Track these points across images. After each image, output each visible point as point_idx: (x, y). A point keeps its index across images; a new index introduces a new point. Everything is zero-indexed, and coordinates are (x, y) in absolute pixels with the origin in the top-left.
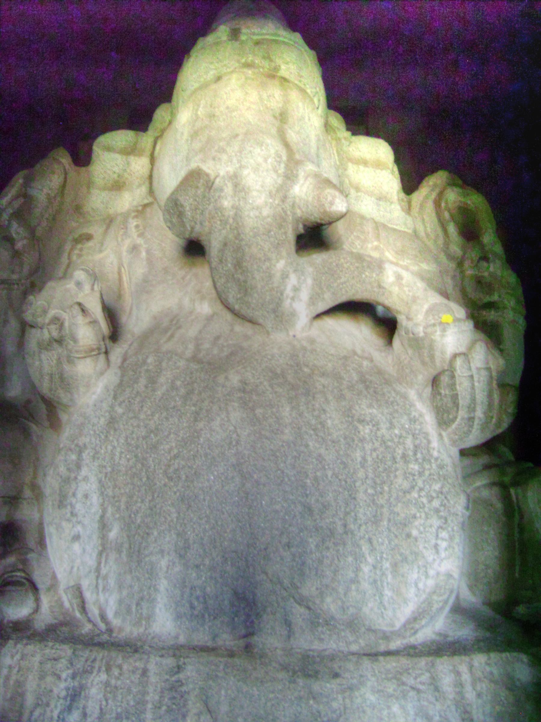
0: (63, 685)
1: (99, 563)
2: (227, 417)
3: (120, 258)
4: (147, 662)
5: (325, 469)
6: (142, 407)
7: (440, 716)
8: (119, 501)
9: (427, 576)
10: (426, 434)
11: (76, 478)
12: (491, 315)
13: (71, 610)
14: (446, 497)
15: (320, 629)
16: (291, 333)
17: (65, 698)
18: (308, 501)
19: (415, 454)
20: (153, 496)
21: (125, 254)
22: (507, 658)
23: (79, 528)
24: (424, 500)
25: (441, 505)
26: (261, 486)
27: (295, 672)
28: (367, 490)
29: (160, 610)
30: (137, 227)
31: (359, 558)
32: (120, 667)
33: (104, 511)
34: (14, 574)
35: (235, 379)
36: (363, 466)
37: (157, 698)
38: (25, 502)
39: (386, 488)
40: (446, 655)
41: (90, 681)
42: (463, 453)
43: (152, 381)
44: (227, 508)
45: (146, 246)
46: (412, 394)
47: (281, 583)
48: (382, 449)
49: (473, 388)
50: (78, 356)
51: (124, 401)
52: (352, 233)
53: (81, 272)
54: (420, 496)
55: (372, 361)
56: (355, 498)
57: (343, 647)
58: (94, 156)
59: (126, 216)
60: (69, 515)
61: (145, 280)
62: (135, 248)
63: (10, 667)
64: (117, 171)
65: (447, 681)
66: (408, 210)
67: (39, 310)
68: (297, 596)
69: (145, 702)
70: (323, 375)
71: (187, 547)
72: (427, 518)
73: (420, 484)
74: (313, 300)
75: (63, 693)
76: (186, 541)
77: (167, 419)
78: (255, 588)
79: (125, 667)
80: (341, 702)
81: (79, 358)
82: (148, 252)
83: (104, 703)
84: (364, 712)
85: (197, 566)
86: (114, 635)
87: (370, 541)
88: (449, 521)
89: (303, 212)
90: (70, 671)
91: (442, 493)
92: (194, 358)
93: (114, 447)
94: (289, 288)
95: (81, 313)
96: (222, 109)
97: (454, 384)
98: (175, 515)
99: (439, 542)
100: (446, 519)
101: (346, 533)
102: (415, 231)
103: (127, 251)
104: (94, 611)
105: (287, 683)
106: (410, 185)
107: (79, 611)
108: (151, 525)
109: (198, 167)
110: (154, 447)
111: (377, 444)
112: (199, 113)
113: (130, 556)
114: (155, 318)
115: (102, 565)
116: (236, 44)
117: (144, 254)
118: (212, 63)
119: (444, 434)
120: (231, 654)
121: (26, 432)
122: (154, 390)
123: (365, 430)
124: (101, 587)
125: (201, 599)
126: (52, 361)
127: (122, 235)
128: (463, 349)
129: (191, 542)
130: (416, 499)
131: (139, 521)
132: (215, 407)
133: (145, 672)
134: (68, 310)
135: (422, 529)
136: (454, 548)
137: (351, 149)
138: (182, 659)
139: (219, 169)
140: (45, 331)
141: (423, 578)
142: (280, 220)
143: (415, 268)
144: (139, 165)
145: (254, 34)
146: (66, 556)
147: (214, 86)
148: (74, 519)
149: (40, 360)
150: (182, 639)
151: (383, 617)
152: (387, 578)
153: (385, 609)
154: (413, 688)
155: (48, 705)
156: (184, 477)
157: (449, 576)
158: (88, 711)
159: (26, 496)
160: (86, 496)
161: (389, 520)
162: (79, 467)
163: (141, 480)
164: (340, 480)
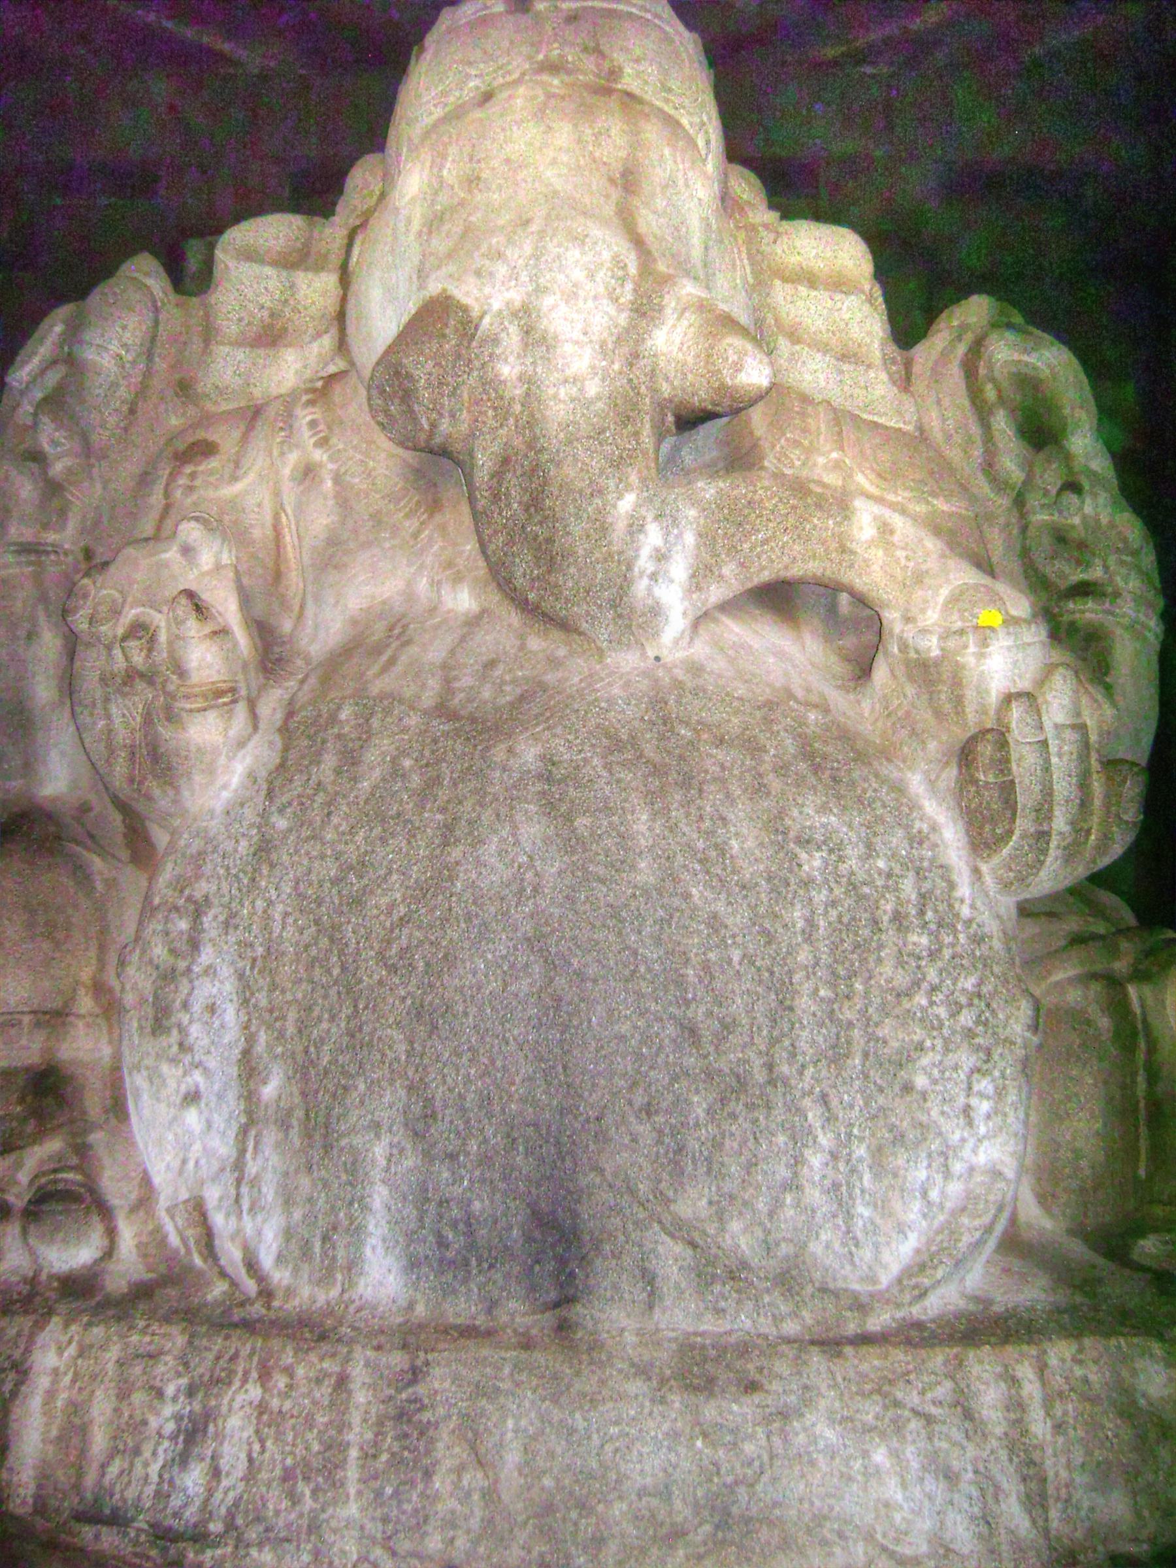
0: (168, 1410)
1: (242, 1152)
2: (514, 835)
3: (277, 494)
4: (347, 1359)
5: (726, 946)
6: (329, 814)
7: (976, 1472)
8: (284, 1018)
9: (947, 1174)
11: (189, 970)
12: (1087, 611)
13: (183, 1251)
14: (988, 1005)
15: (717, 1288)
16: (651, 653)
17: (173, 1438)
18: (690, 1014)
19: (922, 913)
20: (355, 1006)
22: (1119, 1348)
23: (198, 1077)
24: (942, 1012)
25: (978, 1022)
26: (589, 984)
27: (663, 1381)
28: (816, 990)
29: (374, 1248)
30: (313, 424)
31: (800, 1136)
32: (289, 1371)
33: (251, 1040)
34: (60, 1176)
35: (529, 754)
36: (808, 938)
37: (369, 1435)
38: (81, 1024)
39: (858, 986)
40: (988, 1343)
41: (225, 1402)
42: (1025, 911)
43: (350, 759)
44: (516, 1032)
46: (916, 782)
47: (632, 1192)
48: (848, 902)
49: (1047, 768)
50: (188, 706)
51: (290, 804)
52: (784, 434)
53: (193, 524)
54: (932, 1003)
55: (827, 711)
56: (791, 1009)
57: (765, 1325)
58: (218, 272)
59: (289, 402)
60: (175, 1048)
61: (333, 541)
62: (308, 472)
63: (56, 1372)
65: (990, 1400)
66: (905, 382)
67: (103, 609)
68: (667, 1218)
69: (344, 1447)
70: (720, 742)
71: (430, 1115)
72: (947, 1050)
73: (932, 975)
75: (170, 1426)
76: (429, 1101)
77: (383, 840)
78: (578, 1201)
79: (300, 1371)
80: (764, 1442)
81: (191, 711)
82: (337, 479)
83: (257, 1447)
84: (812, 1463)
85: (453, 1157)
86: (276, 1304)
87: (824, 1099)
88: (996, 1057)
89: (674, 388)
90: (184, 1381)
91: (979, 996)
92: (443, 710)
93: (270, 903)
94: (645, 552)
96: (495, 163)
97: (1008, 761)
98: (402, 1047)
99: (974, 1101)
100: (989, 1054)
101: (772, 1082)
103: (292, 479)
104: (231, 1254)
105: (647, 1404)
106: (908, 326)
107: (200, 1253)
108: (353, 1069)
109: (445, 290)
110: (357, 902)
111: (838, 891)
113: (308, 1135)
114: (354, 622)
115: (249, 1156)
116: (525, 20)
117: (329, 483)
119: (984, 868)
120: (527, 1344)
122: (355, 779)
123: (813, 862)
124: (246, 1204)
125: (461, 1226)
126: (134, 719)
127: (282, 443)
128: (1025, 685)
129: (438, 1104)
130: (923, 1009)
132: (487, 816)
133: (342, 1381)
134: (165, 609)
135: (936, 1072)
136: (1005, 1115)
137: (779, 251)
138: (421, 1354)
139: (490, 295)
141: (939, 1178)
142: (624, 410)
143: (920, 508)
144: (316, 289)
146: (171, 1137)
148: (188, 1059)
149: (109, 717)
151: (852, 1263)
152: (861, 1179)
153: (857, 1246)
154: (916, 1413)
155: (137, 1451)
157: (996, 1174)
158: (224, 1464)
159: (83, 1011)
160: (212, 1009)
161: (866, 1055)
162: (195, 945)
163: (329, 971)
164: (759, 970)
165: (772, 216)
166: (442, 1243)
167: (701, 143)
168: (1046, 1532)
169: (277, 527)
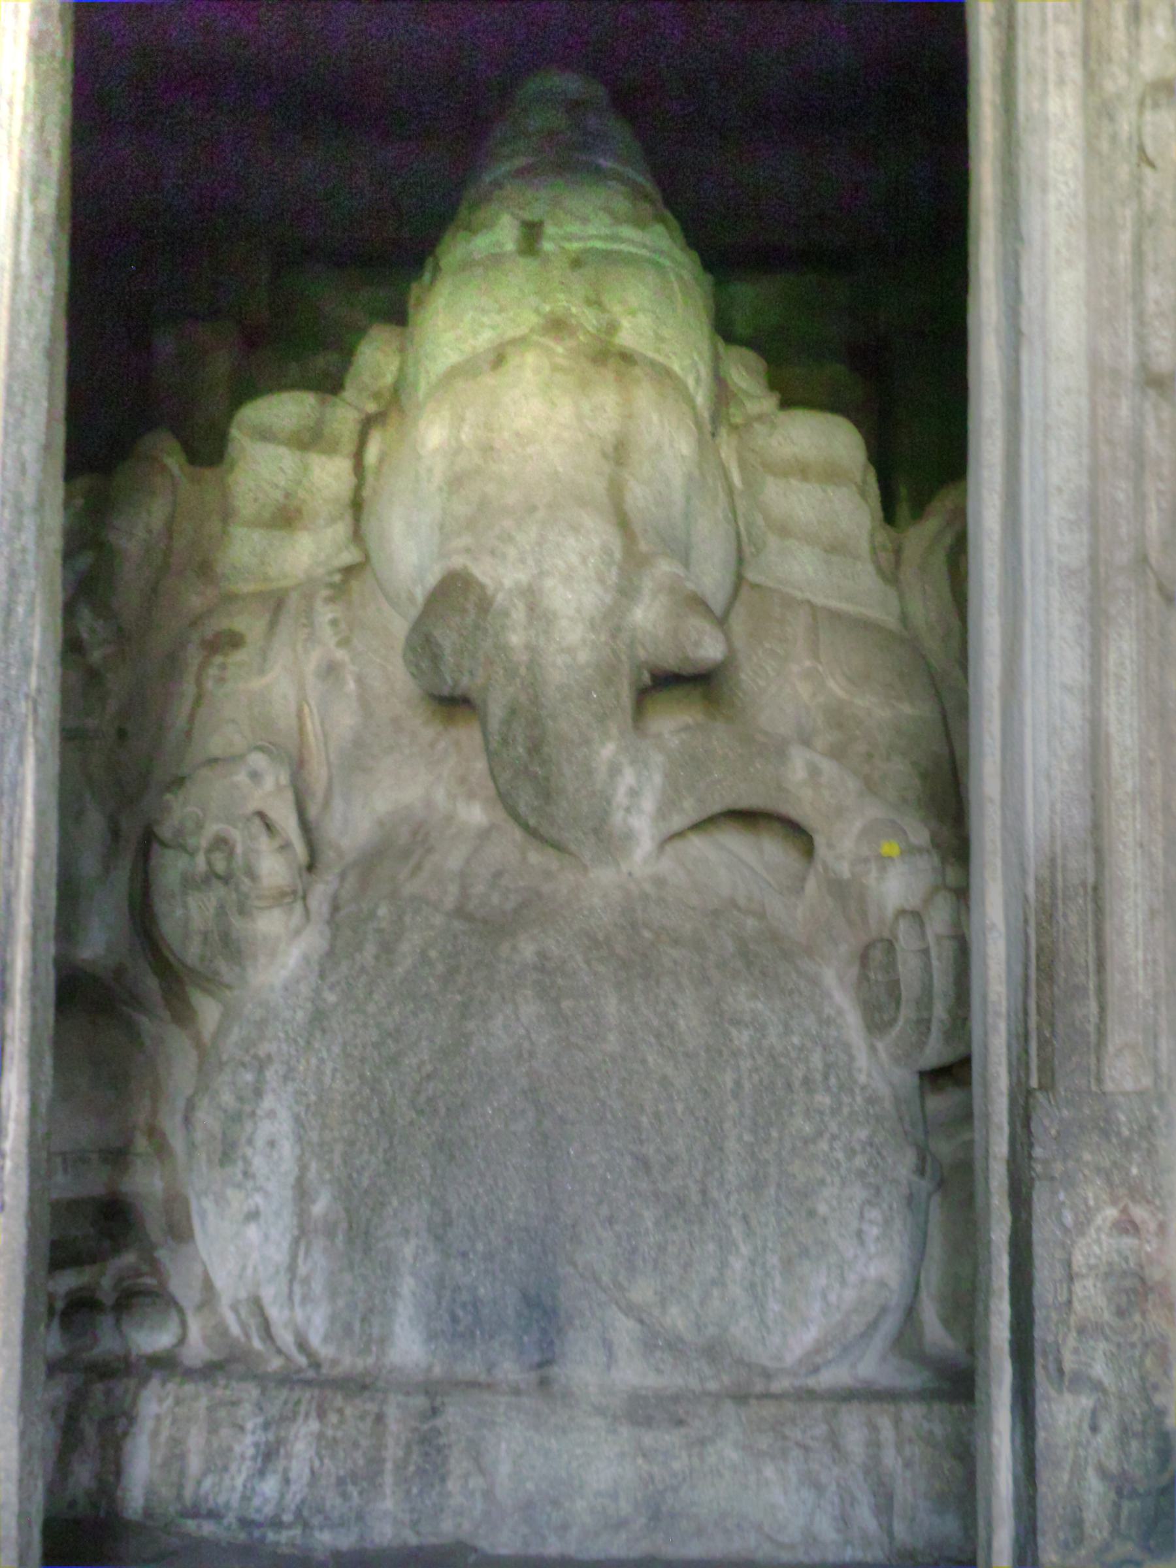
0: (249, 1439)
1: (294, 1257)
4: (384, 1402)
6: (371, 993)
7: (839, 1485)
8: (331, 1151)
9: (843, 1282)
10: (847, 1048)
11: (253, 1114)
13: (243, 1339)
15: (658, 1354)
16: (624, 868)
17: (254, 1458)
18: (644, 1150)
19: (826, 1077)
20: (391, 1143)
21: (311, 680)
23: (258, 1199)
24: (840, 1155)
25: (870, 1163)
27: (615, 1417)
29: (402, 1326)
30: (334, 623)
31: (726, 1246)
32: (340, 1411)
33: (303, 1168)
35: (528, 951)
36: (736, 1095)
37: (400, 1453)
38: (139, 1162)
39: (774, 1134)
41: (292, 1433)
43: (387, 948)
45: (355, 669)
46: (829, 977)
47: (597, 1281)
49: (927, 968)
51: (338, 983)
54: (832, 1148)
55: (761, 915)
56: (721, 1149)
57: (694, 1383)
58: (233, 450)
59: (308, 589)
60: (240, 1176)
61: (358, 743)
62: (331, 670)
63: (158, 1418)
64: (282, 483)
65: (854, 1439)
69: (383, 1461)
70: (676, 942)
71: (448, 1223)
73: (833, 1127)
74: (662, 813)
75: (251, 1452)
76: (446, 1212)
77: (415, 1014)
79: (348, 1411)
82: (360, 680)
83: (317, 1463)
84: (721, 1475)
85: (464, 1255)
86: (324, 1371)
87: (745, 1218)
90: (260, 1420)
91: (871, 1145)
92: (460, 912)
93: (322, 1061)
95: (263, 830)
96: (506, 435)
98: (427, 1173)
99: (865, 1227)
100: (878, 1190)
102: (904, 618)
104: (286, 1339)
105: (603, 1434)
107: (261, 1338)
109: (465, 567)
110: (394, 1061)
111: (760, 1061)
112: (463, 437)
113: (350, 1241)
114: (381, 823)
115: (300, 1260)
116: (532, 264)
117: (351, 686)
118: (484, 311)
119: (880, 1046)
120: (517, 1392)
121: (133, 1033)
122: (391, 964)
123: (742, 1038)
124: (297, 1299)
125: (470, 1308)
127: (306, 640)
128: (914, 903)
129: (454, 1215)
131: (365, 1182)
132: (495, 997)
133: (380, 1418)
134: (240, 825)
135: (835, 1203)
139: (501, 575)
140: (201, 859)
141: (837, 1285)
142: (607, 673)
145: (570, 238)
146: (232, 1248)
147: (489, 380)
148: (250, 1184)
149: (185, 906)
150: (437, 1370)
151: (764, 1344)
153: (769, 1332)
154: (798, 1444)
155: (226, 1468)
156: (443, 1111)
157: (882, 1284)
158: (293, 1475)
160: (272, 1144)
161: (779, 1186)
162: (258, 1093)
163: (370, 1115)
165: (768, 403)
166: (455, 1319)
167: (691, 382)
168: (890, 1534)
169: (300, 715)
